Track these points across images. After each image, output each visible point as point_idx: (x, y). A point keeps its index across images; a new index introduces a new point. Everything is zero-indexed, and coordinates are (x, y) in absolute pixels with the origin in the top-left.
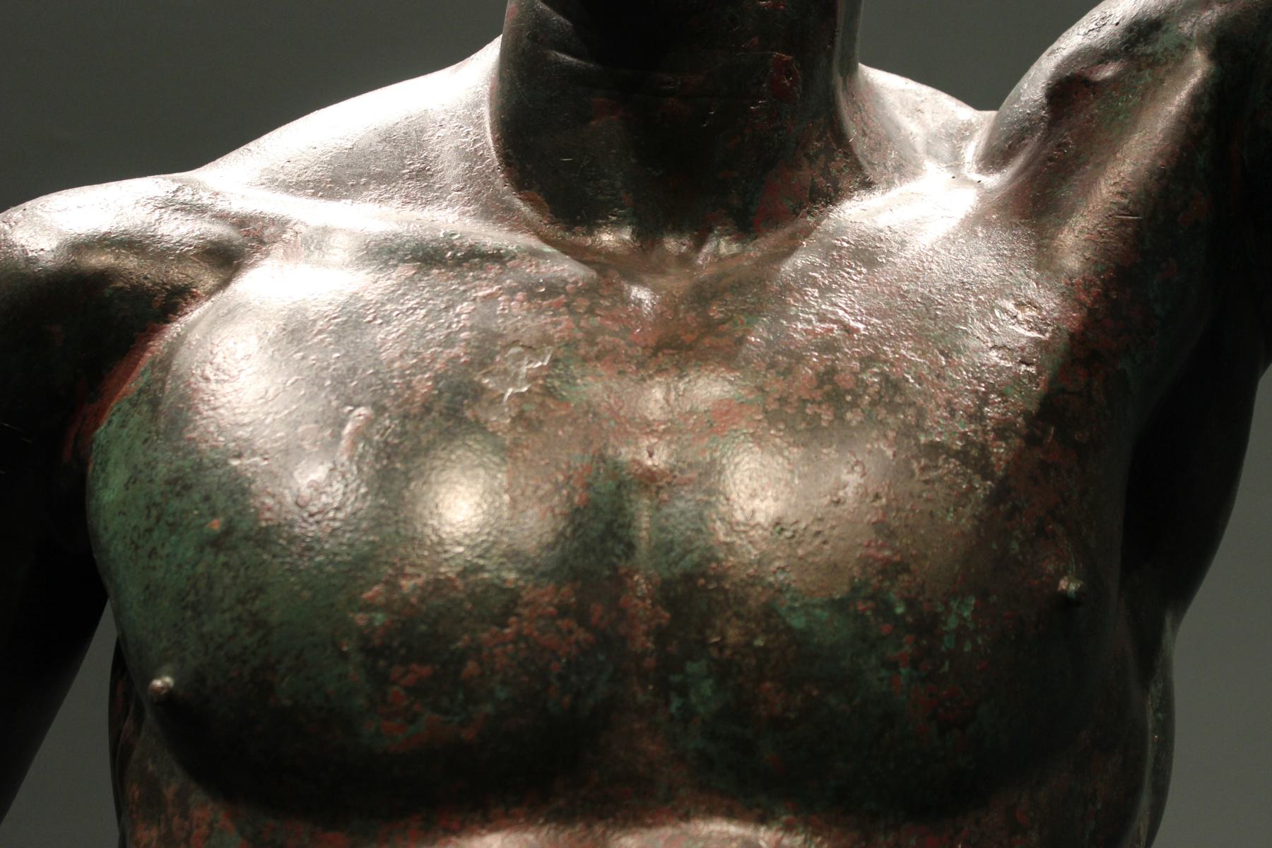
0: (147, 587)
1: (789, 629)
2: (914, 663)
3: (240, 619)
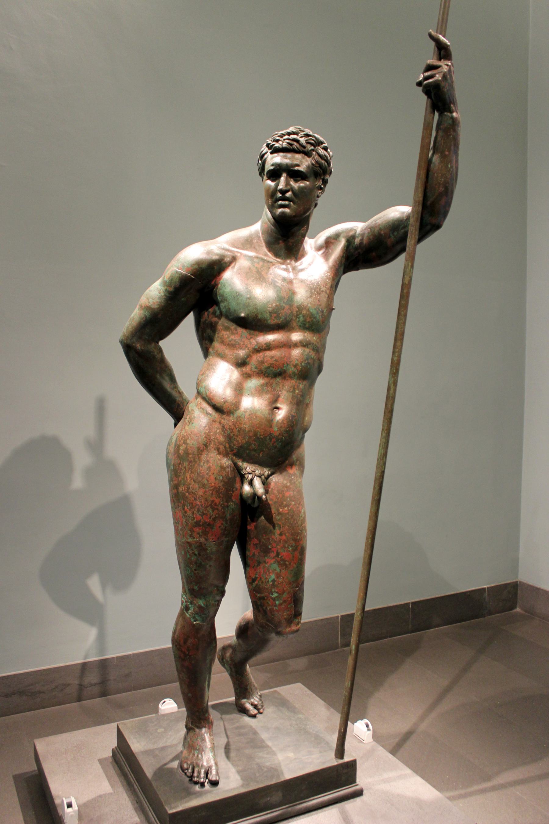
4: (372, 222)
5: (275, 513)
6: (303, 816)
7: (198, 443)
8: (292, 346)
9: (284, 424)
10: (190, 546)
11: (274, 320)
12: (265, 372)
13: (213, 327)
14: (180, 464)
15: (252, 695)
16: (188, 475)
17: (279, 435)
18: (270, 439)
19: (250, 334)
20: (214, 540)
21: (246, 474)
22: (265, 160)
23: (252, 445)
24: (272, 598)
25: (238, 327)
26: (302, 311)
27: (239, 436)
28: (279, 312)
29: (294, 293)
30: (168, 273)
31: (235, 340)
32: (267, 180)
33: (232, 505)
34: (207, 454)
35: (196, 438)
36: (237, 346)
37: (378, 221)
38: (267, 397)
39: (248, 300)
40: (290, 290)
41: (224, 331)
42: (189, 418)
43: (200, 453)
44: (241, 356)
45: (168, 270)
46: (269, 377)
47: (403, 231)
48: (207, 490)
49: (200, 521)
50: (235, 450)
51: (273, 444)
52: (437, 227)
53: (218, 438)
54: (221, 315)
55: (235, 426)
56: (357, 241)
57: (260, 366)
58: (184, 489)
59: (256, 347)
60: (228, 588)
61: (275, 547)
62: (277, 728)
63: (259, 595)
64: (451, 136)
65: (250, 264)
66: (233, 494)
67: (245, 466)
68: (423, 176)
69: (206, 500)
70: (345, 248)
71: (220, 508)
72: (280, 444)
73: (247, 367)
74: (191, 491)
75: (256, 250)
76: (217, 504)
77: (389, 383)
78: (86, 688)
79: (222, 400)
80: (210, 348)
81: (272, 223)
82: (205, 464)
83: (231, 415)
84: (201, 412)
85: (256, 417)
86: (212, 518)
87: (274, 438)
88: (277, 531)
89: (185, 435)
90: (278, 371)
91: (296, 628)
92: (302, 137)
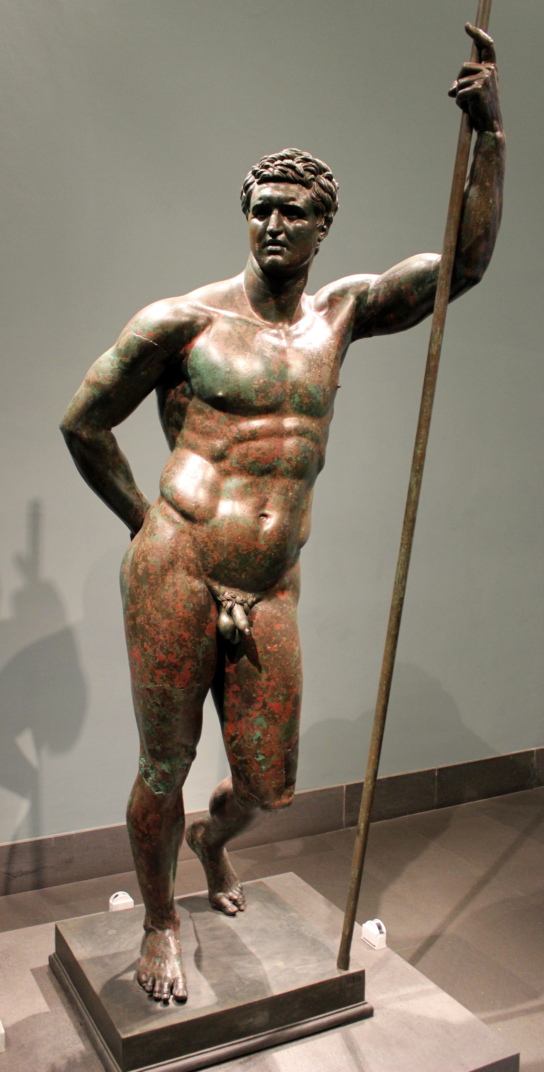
1: (309, 390)
2: (323, 396)
3: (235, 385)
4: (390, 274)
5: (261, 652)
6: (296, 1043)
7: (162, 560)
8: (284, 435)
9: (274, 536)
10: (150, 694)
11: (261, 401)
12: (250, 468)
13: (182, 410)
14: (138, 587)
15: (230, 888)
16: (148, 601)
17: (267, 550)
18: (256, 556)
19: (230, 419)
20: (182, 686)
21: (223, 601)
22: (251, 192)
23: (232, 563)
24: (257, 762)
25: (214, 409)
26: (297, 389)
27: (215, 552)
28: (268, 391)
29: (287, 366)
30: (123, 339)
31: (210, 427)
32: (253, 218)
33: (206, 641)
34: (174, 575)
35: (159, 554)
36: (213, 434)
37: (397, 273)
38: (252, 500)
39: (227, 374)
40: (282, 362)
41: (196, 414)
42: (150, 528)
43: (165, 573)
44: (217, 448)
45: (124, 335)
46: (254, 475)
47: (429, 286)
48: (173, 621)
49: (164, 662)
50: (209, 569)
51: (259, 562)
52: (475, 281)
53: (188, 555)
54: (192, 394)
55: (210, 538)
56: (370, 298)
57: (243, 461)
58: (143, 619)
59: (238, 436)
60: (200, 748)
61: (262, 696)
62: (263, 930)
63: (239, 758)
64: (494, 163)
65: (231, 328)
66: (207, 627)
67: (223, 590)
68: (456, 214)
69: (172, 634)
70: (354, 307)
71: (190, 645)
72: (268, 562)
73: (226, 462)
74: (153, 622)
75: (238, 309)
76: (187, 639)
77: (410, 484)
78: (16, 877)
79: (193, 505)
80: (177, 436)
81: (260, 274)
82: (171, 588)
83: (205, 524)
84: (165, 519)
85: (238, 527)
86: (179, 657)
87: (260, 553)
88: (264, 675)
89: (145, 549)
90: (266, 466)
91: (288, 801)
92: (298, 162)
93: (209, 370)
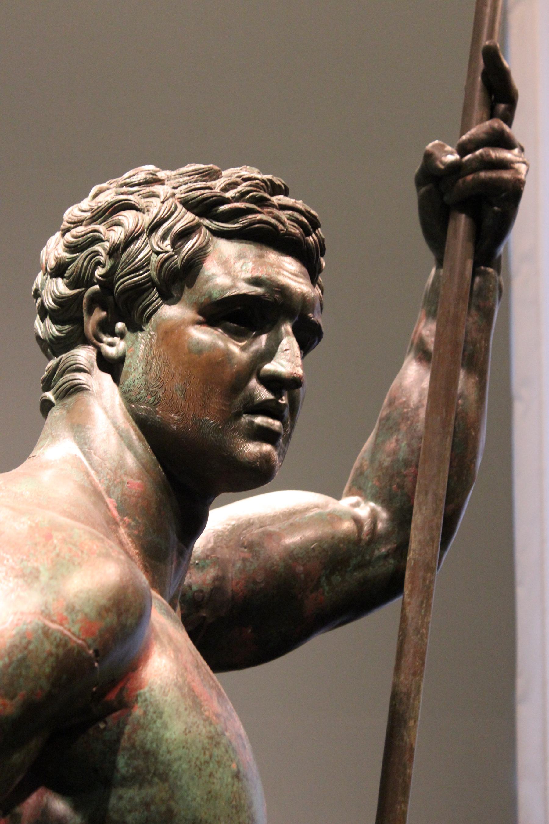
0: (210, 792)
93: (198, 763)
